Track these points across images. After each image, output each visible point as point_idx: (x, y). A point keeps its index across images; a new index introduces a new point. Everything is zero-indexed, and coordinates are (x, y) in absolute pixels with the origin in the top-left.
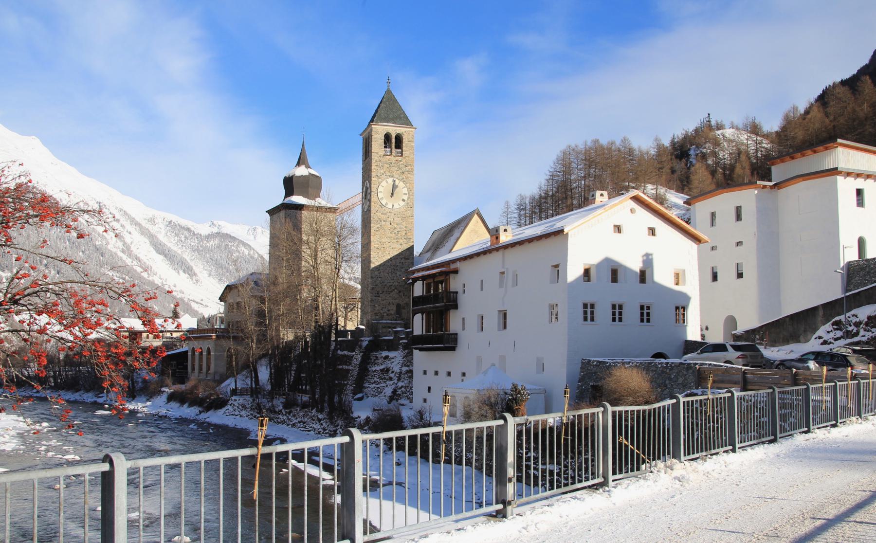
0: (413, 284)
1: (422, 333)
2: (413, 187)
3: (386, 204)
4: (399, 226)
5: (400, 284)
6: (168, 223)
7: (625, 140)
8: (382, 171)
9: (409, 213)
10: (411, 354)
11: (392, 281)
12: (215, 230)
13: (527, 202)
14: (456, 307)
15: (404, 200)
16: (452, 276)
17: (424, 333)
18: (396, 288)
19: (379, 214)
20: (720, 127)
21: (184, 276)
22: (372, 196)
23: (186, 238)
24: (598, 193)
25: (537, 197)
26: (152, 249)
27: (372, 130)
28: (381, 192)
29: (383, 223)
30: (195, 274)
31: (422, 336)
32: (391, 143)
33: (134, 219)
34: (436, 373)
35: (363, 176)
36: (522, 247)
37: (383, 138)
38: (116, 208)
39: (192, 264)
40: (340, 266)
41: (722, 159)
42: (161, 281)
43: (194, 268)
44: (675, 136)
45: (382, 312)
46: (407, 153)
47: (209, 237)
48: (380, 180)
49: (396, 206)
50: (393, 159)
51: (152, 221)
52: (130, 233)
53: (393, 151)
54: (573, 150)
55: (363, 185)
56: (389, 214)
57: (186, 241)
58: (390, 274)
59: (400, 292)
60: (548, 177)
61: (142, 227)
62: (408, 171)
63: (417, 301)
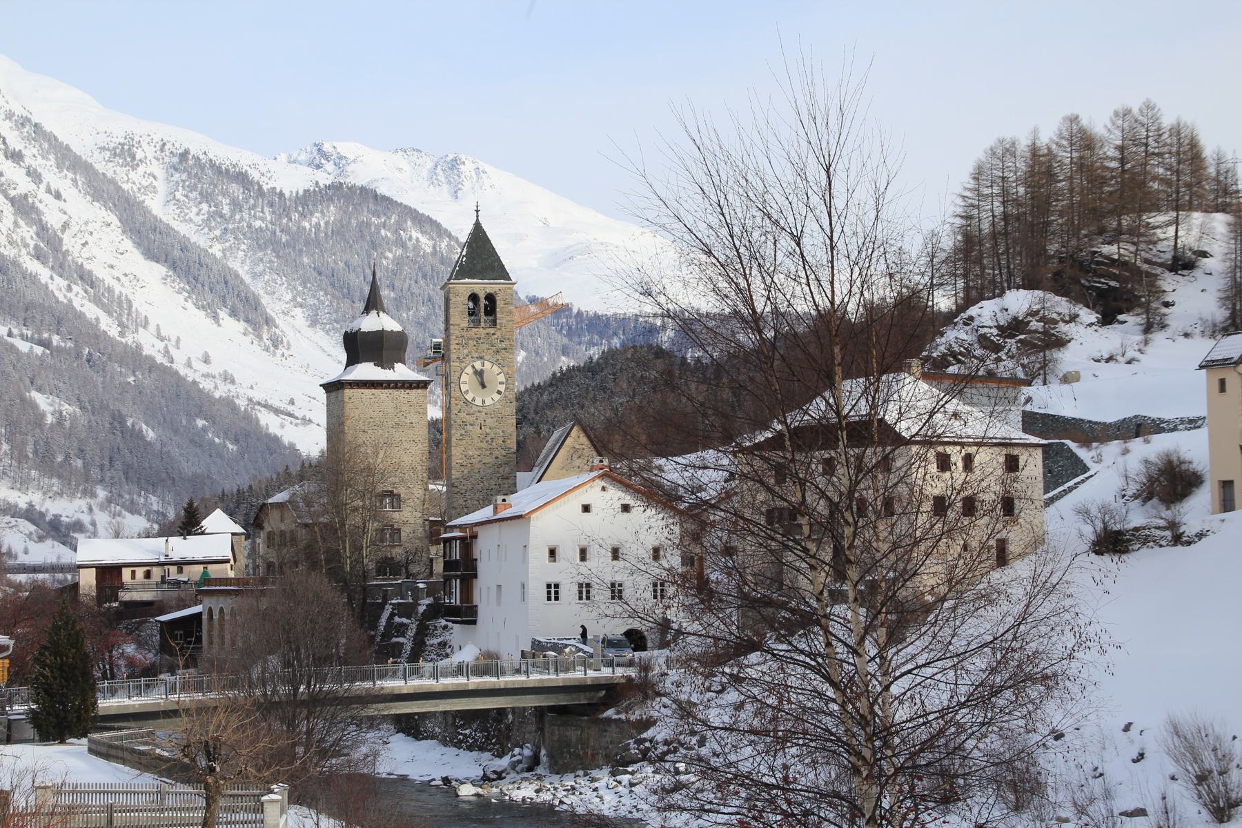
6: (176, 160)
12: (325, 179)
21: (232, 327)
23: (236, 205)
26: (128, 244)
30: (269, 321)
33: (67, 148)
39: (257, 288)
42: (161, 345)
43: (265, 300)
47: (309, 200)
51: (126, 153)
52: (58, 196)
57: (237, 217)
61: (96, 173)
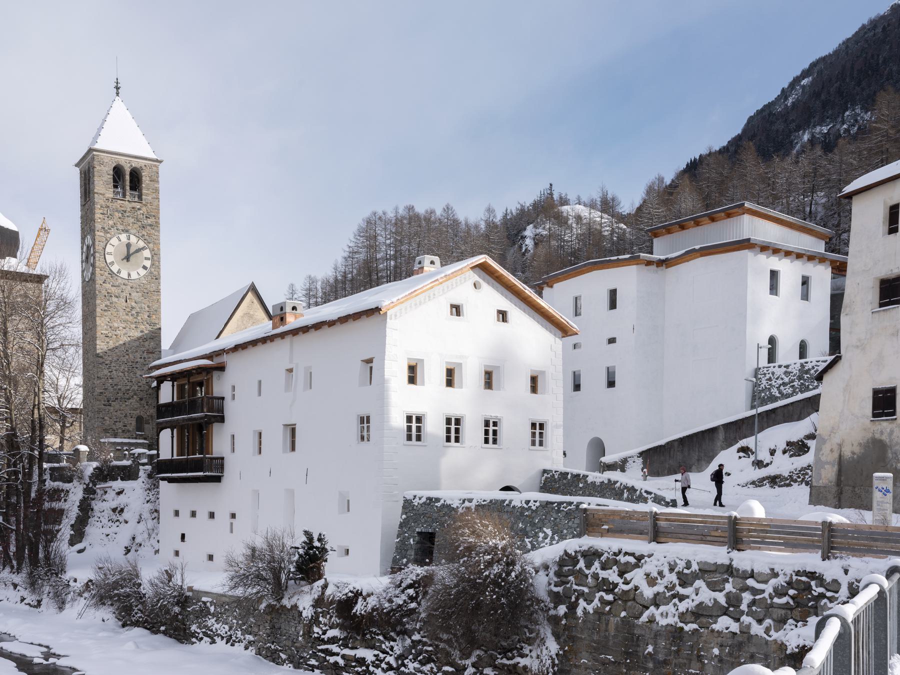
0: (158, 388)
1: (172, 456)
2: (159, 249)
3: (119, 272)
4: (139, 305)
5: (142, 388)
7: (447, 209)
8: (111, 222)
9: (153, 287)
10: (156, 486)
11: (130, 384)
13: (319, 287)
14: (222, 419)
15: (145, 268)
16: (215, 374)
17: (175, 457)
18: (135, 394)
19: (108, 286)
20: (564, 202)
22: (97, 259)
24: (427, 258)
25: (332, 280)
27: (93, 158)
28: (110, 254)
29: (114, 299)
31: (171, 461)
32: (124, 181)
34: (193, 514)
35: (82, 229)
36: (319, 332)
37: (112, 172)
40: (44, 357)
41: (569, 241)
44: (509, 211)
45: (114, 427)
46: (150, 198)
48: (109, 235)
49: (134, 276)
50: (128, 206)
53: (128, 194)
54: (380, 218)
55: (83, 242)
56: (124, 287)
58: (126, 374)
59: (141, 399)
60: (346, 254)
62: (150, 225)
63: (164, 410)
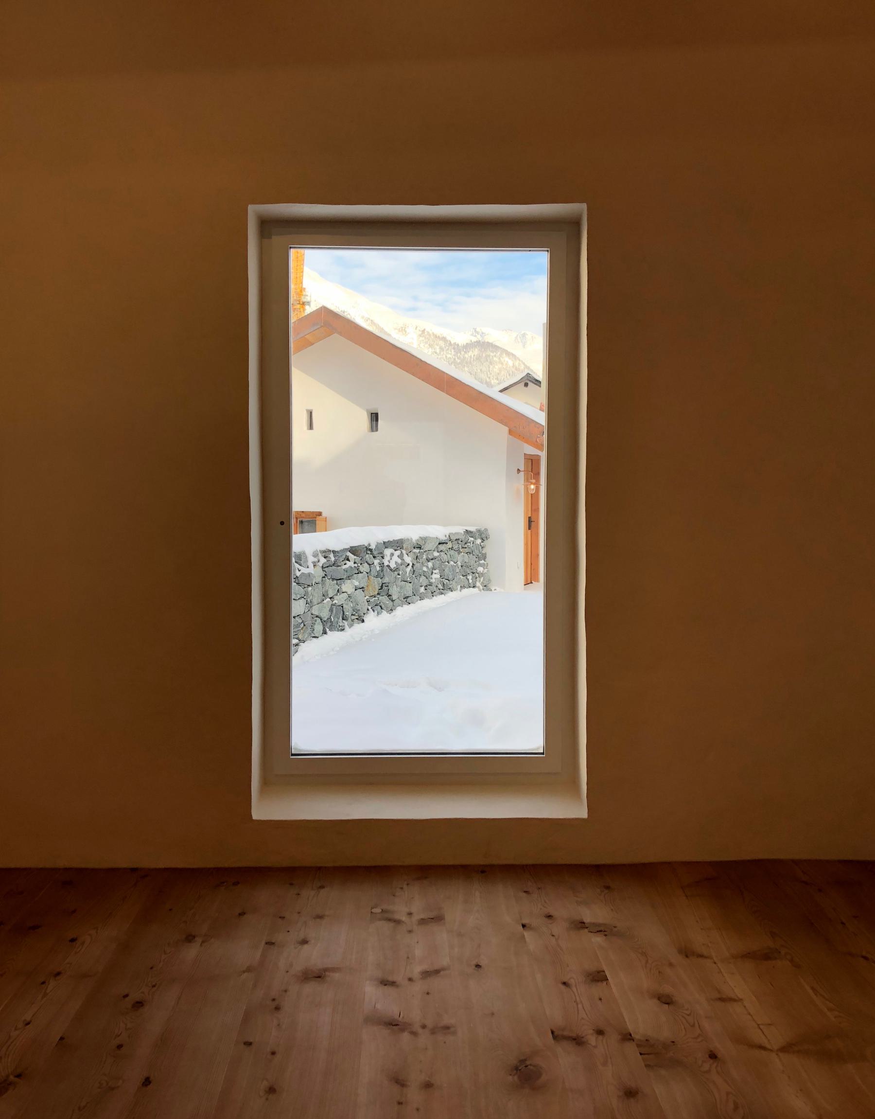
6: (421, 333)
12: (474, 339)
23: (441, 349)
33: (383, 329)
38: (363, 317)
47: (468, 347)
51: (403, 330)
57: (442, 353)
